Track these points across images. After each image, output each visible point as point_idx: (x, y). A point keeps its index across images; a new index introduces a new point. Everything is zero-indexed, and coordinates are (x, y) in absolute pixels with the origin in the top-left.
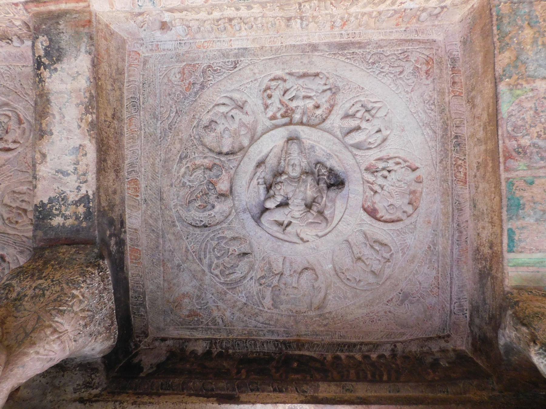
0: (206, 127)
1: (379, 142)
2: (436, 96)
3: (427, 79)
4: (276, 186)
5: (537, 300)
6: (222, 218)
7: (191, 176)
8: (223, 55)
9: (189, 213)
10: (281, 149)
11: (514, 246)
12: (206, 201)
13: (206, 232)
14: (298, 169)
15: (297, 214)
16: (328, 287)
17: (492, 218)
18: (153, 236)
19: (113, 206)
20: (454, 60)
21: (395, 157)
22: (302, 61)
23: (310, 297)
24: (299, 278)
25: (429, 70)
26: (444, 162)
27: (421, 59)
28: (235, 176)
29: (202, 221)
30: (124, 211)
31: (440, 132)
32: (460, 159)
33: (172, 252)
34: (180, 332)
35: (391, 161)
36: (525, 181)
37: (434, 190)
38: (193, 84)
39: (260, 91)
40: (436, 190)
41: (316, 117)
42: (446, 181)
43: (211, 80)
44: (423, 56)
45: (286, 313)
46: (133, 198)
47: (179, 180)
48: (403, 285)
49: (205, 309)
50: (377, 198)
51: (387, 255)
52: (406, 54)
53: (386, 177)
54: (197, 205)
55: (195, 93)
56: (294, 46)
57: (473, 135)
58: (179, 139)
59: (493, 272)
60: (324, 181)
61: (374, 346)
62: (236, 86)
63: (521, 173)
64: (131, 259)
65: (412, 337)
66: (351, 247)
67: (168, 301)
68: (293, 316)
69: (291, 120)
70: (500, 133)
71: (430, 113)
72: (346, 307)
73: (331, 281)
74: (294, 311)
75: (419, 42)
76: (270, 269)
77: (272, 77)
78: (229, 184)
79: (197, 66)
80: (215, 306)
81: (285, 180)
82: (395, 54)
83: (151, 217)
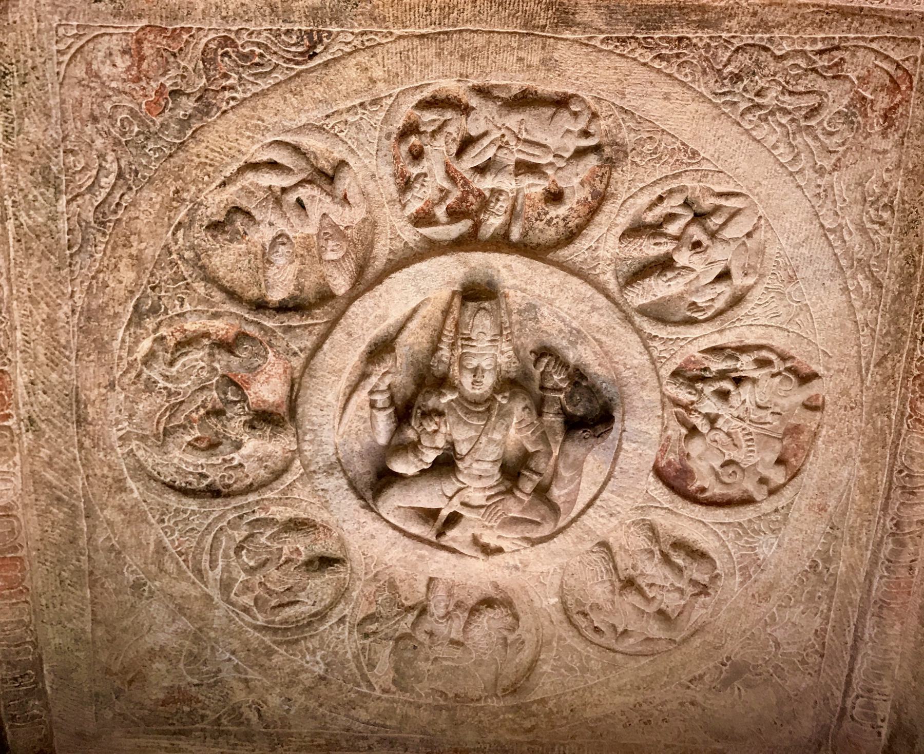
0: (215, 227)
1: (720, 304)
2: (900, 184)
7: (171, 364)
9: (165, 457)
10: (441, 305)
12: (217, 433)
13: (217, 507)
14: (488, 381)
16: (542, 645)
18: (58, 513)
21: (760, 347)
22: (522, 54)
23: (494, 667)
25: (894, 108)
26: (889, 364)
28: (306, 379)
29: (205, 476)
31: (892, 285)
33: (116, 552)
37: (849, 431)
38: (172, 93)
39: (388, 137)
40: (854, 431)
41: (549, 222)
42: (885, 411)
43: (232, 88)
44: (885, 65)
45: (430, 700)
47: (134, 374)
48: (733, 648)
49: (210, 686)
50: (696, 447)
51: (704, 578)
52: (837, 55)
53: (724, 395)
54: (189, 438)
55: (180, 121)
58: (131, 256)
60: (557, 407)
62: (315, 115)
68: (448, 709)
71: (876, 232)
72: (584, 690)
73: (553, 636)
74: (450, 695)
77: (427, 93)
78: (286, 388)
79: (185, 36)
80: (240, 680)
81: (449, 404)
82: (804, 53)
83: (50, 464)
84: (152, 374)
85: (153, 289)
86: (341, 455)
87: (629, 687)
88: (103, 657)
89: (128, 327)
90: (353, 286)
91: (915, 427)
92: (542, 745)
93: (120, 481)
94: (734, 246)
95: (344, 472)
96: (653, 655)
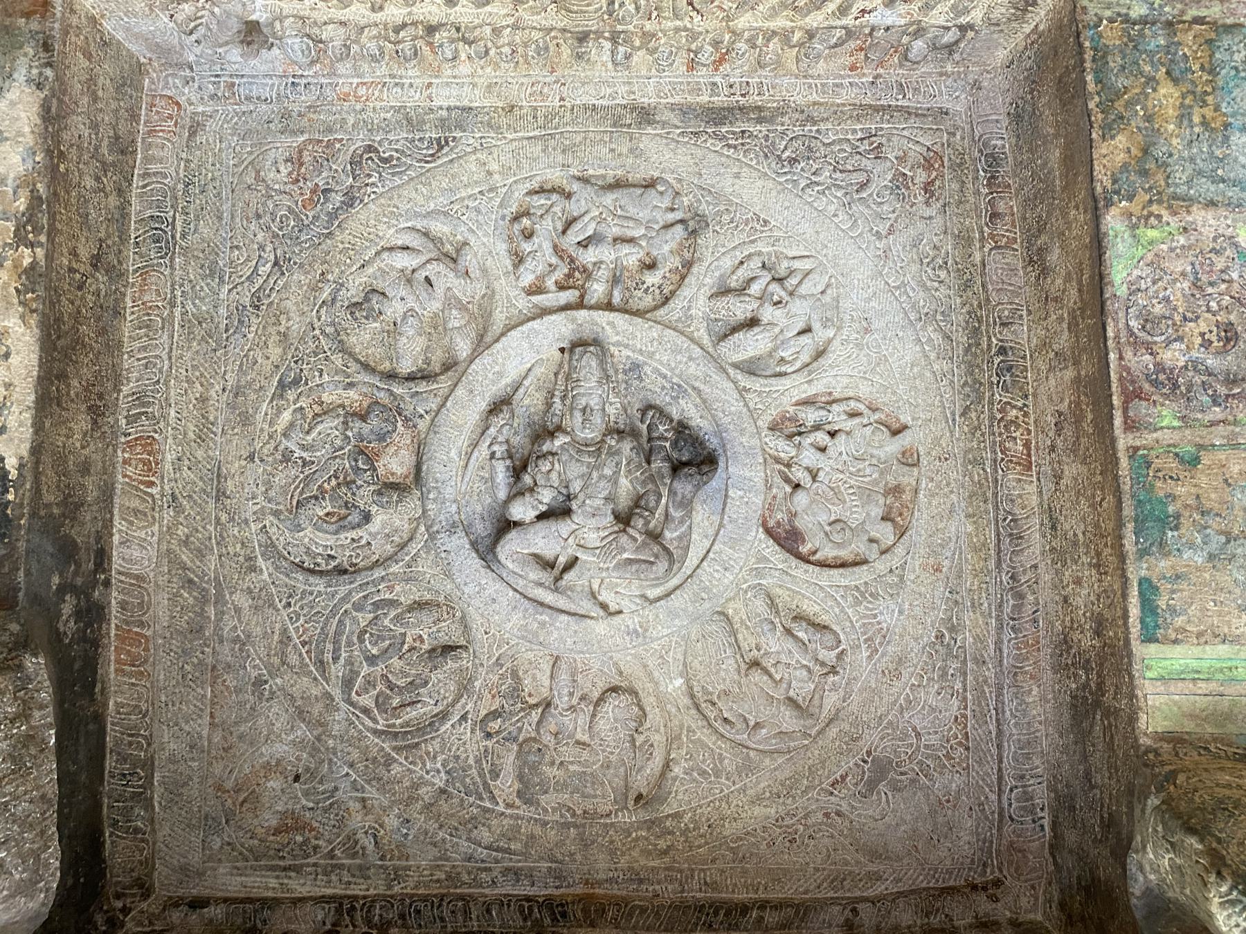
1: (805, 357)
3: (927, 203)
4: (540, 463)
5: (1222, 769)
6: (389, 549)
7: (308, 433)
8: (409, 121)
9: (297, 535)
11: (1157, 626)
12: (346, 503)
15: (593, 538)
17: (1098, 554)
19: (79, 505)
20: (993, 160)
22: (613, 146)
23: (622, 770)
24: (594, 715)
25: (933, 181)
27: (912, 154)
28: (432, 435)
30: (108, 524)
31: (962, 338)
32: (1014, 407)
33: (241, 643)
34: (249, 880)
35: (835, 408)
36: (1177, 455)
37: (948, 484)
38: (325, 191)
39: (503, 218)
41: (646, 291)
43: (373, 184)
45: (557, 817)
46: (137, 489)
47: (273, 444)
48: (871, 738)
49: (325, 810)
50: (801, 499)
51: (829, 656)
52: (877, 140)
53: (823, 450)
56: (594, 107)
57: (1045, 345)
59: (1108, 698)
61: (797, 913)
63: (1166, 437)
64: (118, 661)
65: (901, 887)
66: (734, 633)
67: (219, 788)
68: (576, 826)
69: (582, 297)
70: (1110, 333)
71: (937, 290)
75: (907, 112)
76: (515, 692)
78: (414, 458)
79: (338, 146)
81: (562, 447)
83: (186, 543)
84: (289, 444)
85: (296, 362)
86: (463, 517)
87: (768, 794)
88: (218, 769)
89: (271, 401)
90: (475, 350)
91: (1008, 469)
92: (681, 871)
93: (251, 559)
94: (810, 302)
95: (467, 534)
96: (789, 752)
